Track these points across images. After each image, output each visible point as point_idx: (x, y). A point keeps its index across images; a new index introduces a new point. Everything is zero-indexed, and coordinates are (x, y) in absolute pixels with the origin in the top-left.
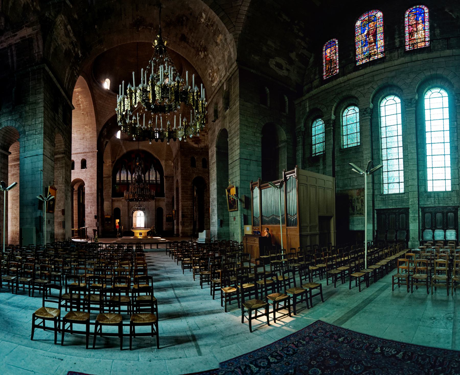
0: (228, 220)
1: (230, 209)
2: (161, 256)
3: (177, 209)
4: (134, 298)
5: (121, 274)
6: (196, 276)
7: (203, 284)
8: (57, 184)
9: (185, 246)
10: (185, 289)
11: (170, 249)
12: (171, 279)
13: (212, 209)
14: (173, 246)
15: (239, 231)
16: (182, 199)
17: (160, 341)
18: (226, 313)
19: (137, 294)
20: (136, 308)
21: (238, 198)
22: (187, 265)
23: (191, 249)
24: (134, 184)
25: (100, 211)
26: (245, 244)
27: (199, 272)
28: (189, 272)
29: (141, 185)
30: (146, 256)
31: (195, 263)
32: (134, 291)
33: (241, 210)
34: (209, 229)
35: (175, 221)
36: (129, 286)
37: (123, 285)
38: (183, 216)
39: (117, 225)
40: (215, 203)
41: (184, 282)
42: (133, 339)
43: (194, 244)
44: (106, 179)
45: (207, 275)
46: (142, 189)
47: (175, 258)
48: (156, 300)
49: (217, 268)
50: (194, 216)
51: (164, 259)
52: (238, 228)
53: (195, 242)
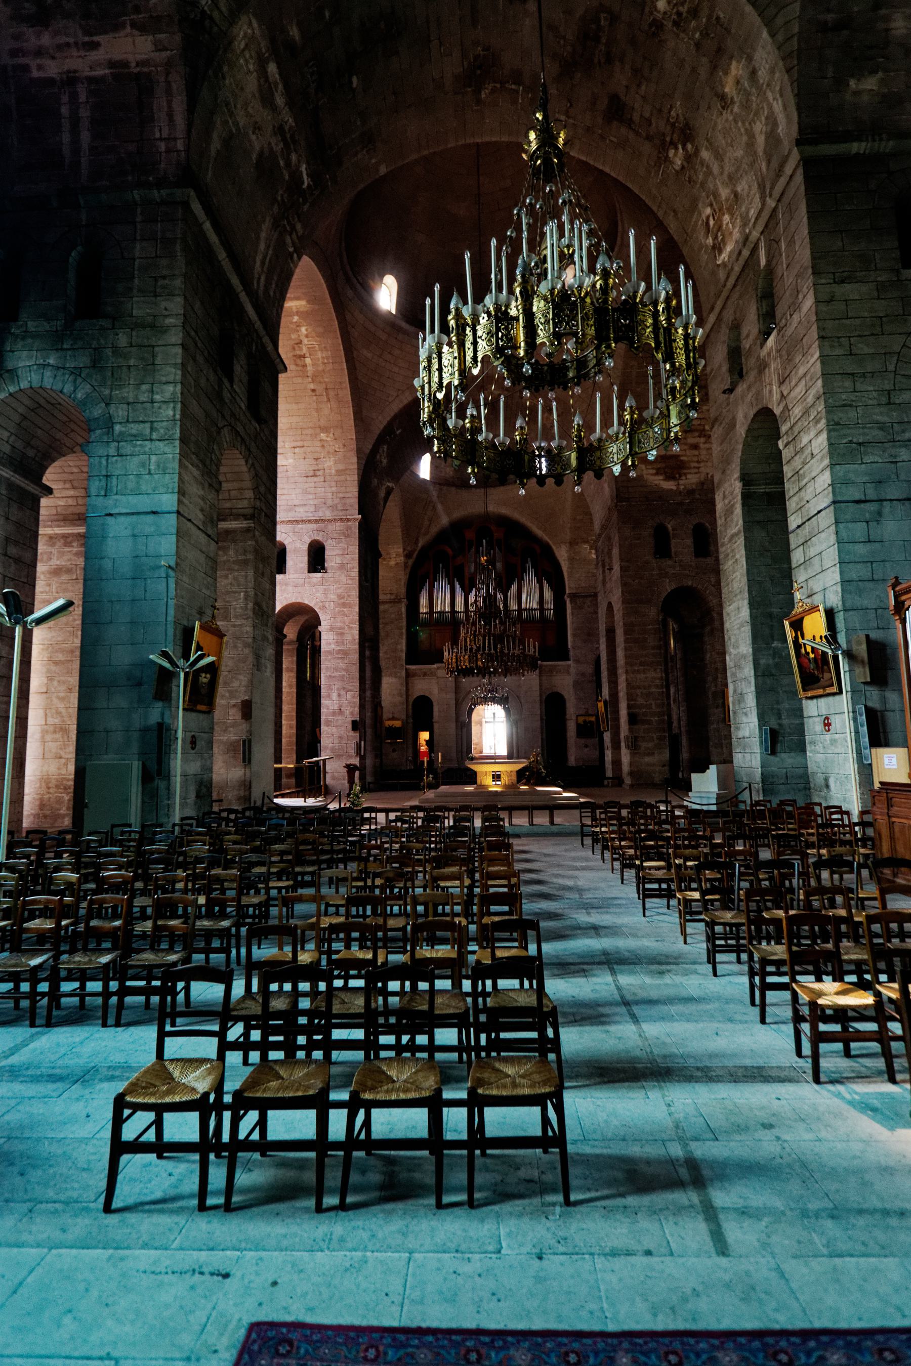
0: (800, 730)
1: (804, 690)
2: (566, 851)
3: (610, 695)
4: (480, 1000)
5: (436, 914)
6: (691, 928)
7: (719, 957)
8: (226, 618)
9: (645, 817)
10: (652, 973)
11: (592, 826)
12: (602, 932)
13: (735, 691)
14: (603, 816)
15: (850, 768)
16: (626, 663)
17: (573, 1171)
18: (816, 1086)
19: (489, 983)
20: (488, 1038)
21: (837, 649)
22: (656, 886)
23: (668, 831)
24: (474, 624)
25: (368, 707)
26: (882, 821)
27: (700, 913)
28: (665, 910)
29: (495, 626)
30: (516, 848)
31: (684, 880)
32: (480, 972)
33: (854, 691)
34: (727, 760)
35: (607, 737)
36: (462, 954)
37: (443, 951)
38: (633, 719)
39: (424, 748)
40: (748, 671)
41: (648, 944)
42: (479, 1162)
43: (677, 813)
44: (386, 606)
45: (731, 925)
46: (499, 639)
47: (614, 860)
48: (555, 1008)
49: (769, 904)
50: (670, 717)
51: (574, 859)
52: (846, 759)
53: (681, 807)
